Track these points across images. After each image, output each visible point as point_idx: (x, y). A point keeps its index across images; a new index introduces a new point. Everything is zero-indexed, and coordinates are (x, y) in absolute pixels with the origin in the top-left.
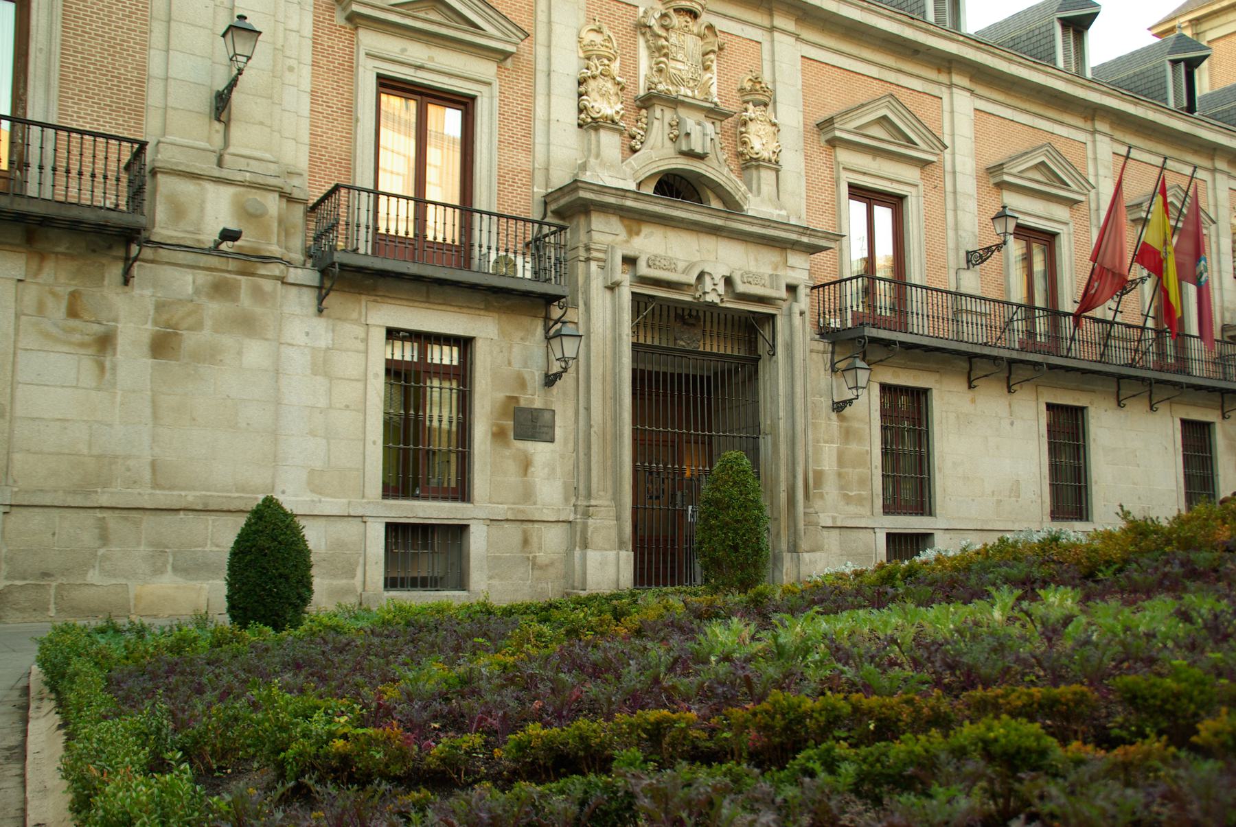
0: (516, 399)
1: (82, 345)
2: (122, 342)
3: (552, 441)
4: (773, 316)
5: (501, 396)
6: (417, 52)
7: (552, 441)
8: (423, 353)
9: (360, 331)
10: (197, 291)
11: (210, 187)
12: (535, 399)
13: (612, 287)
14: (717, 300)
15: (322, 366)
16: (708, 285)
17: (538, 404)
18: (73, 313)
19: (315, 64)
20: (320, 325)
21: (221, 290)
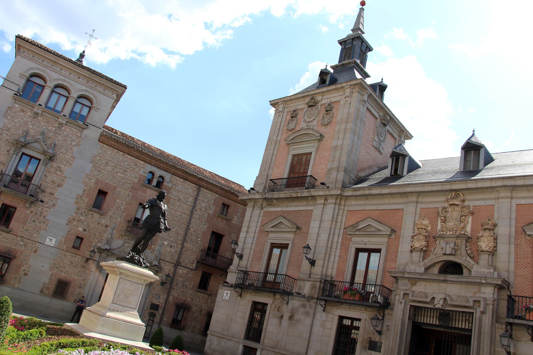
0: (371, 338)
1: (278, 318)
2: (284, 317)
3: (380, 352)
4: (473, 313)
5: (366, 336)
6: (366, 239)
7: (380, 352)
8: (352, 323)
9: (332, 316)
10: (299, 306)
11: (306, 282)
12: (376, 338)
13: (401, 303)
14: (440, 307)
15: (323, 325)
16: (436, 301)
17: (377, 340)
18: (278, 311)
19: (341, 249)
20: (324, 314)
21: (304, 306)
